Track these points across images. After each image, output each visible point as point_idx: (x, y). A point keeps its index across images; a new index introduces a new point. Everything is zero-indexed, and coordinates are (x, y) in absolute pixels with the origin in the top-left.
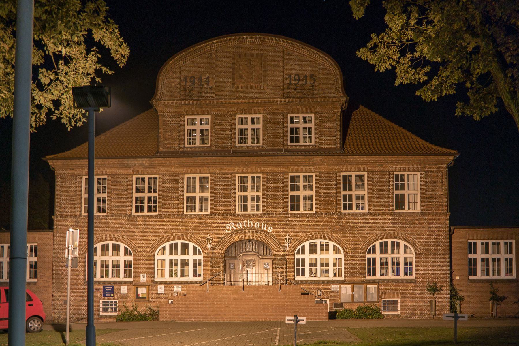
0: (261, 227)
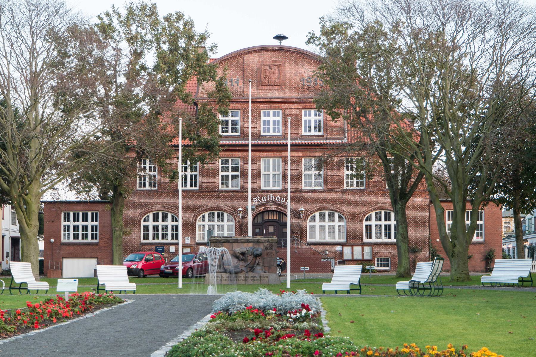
0: (281, 200)
